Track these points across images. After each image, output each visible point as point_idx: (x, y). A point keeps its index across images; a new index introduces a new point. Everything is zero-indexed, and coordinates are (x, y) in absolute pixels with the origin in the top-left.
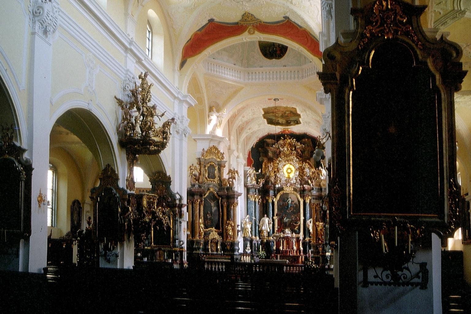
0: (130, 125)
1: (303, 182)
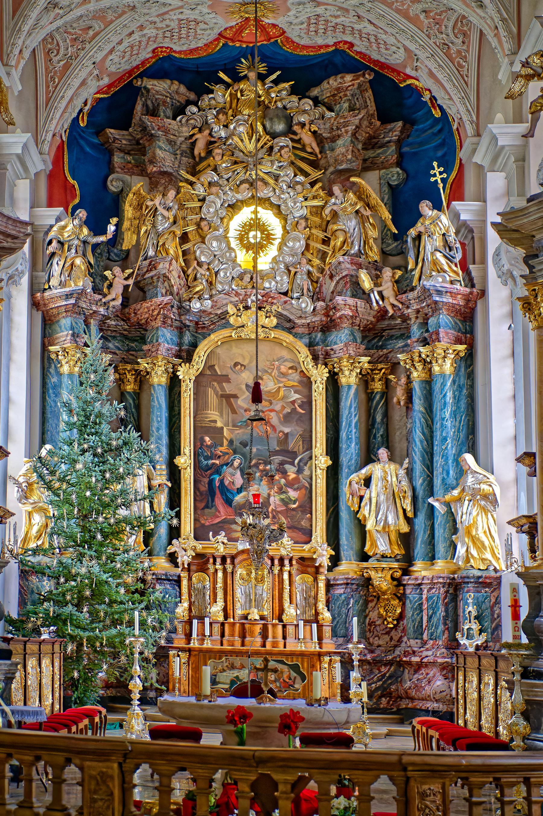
1: (329, 286)
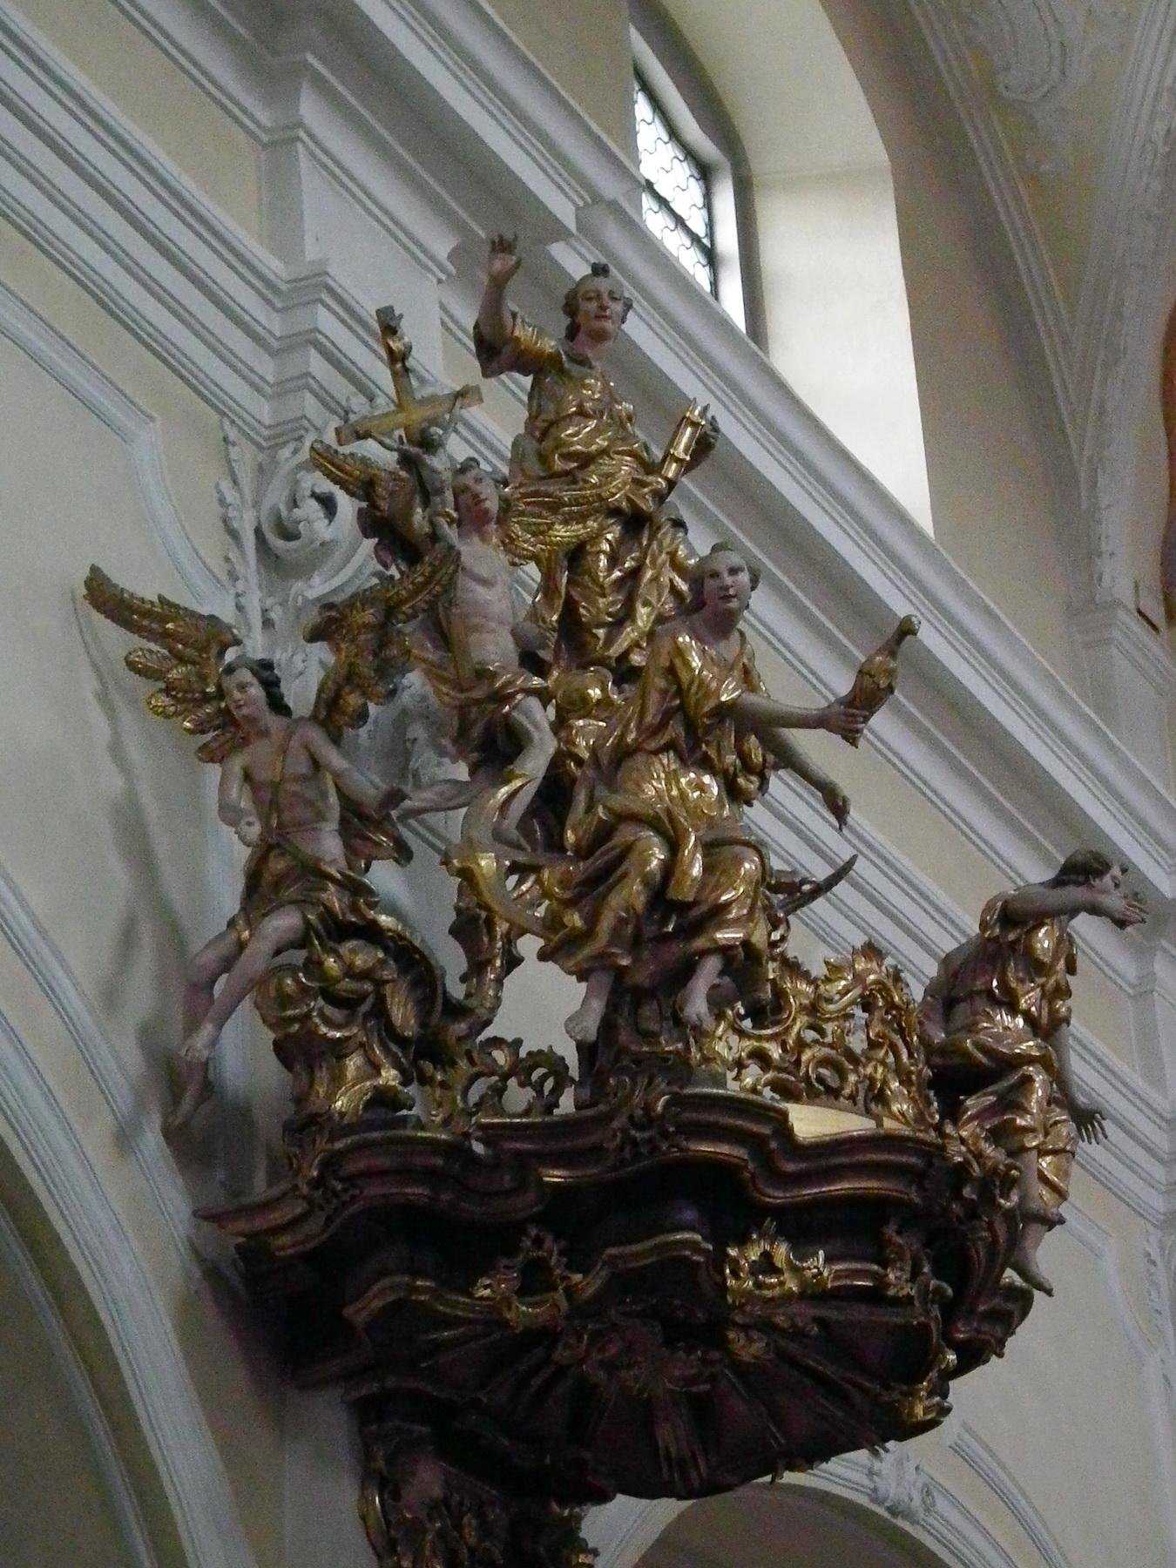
0: (363, 956)
